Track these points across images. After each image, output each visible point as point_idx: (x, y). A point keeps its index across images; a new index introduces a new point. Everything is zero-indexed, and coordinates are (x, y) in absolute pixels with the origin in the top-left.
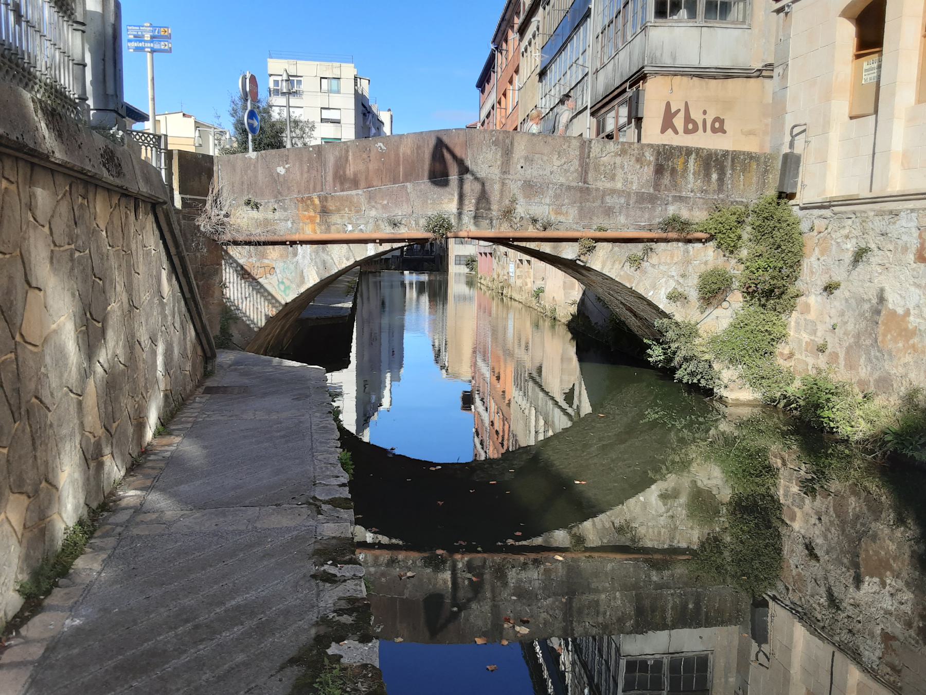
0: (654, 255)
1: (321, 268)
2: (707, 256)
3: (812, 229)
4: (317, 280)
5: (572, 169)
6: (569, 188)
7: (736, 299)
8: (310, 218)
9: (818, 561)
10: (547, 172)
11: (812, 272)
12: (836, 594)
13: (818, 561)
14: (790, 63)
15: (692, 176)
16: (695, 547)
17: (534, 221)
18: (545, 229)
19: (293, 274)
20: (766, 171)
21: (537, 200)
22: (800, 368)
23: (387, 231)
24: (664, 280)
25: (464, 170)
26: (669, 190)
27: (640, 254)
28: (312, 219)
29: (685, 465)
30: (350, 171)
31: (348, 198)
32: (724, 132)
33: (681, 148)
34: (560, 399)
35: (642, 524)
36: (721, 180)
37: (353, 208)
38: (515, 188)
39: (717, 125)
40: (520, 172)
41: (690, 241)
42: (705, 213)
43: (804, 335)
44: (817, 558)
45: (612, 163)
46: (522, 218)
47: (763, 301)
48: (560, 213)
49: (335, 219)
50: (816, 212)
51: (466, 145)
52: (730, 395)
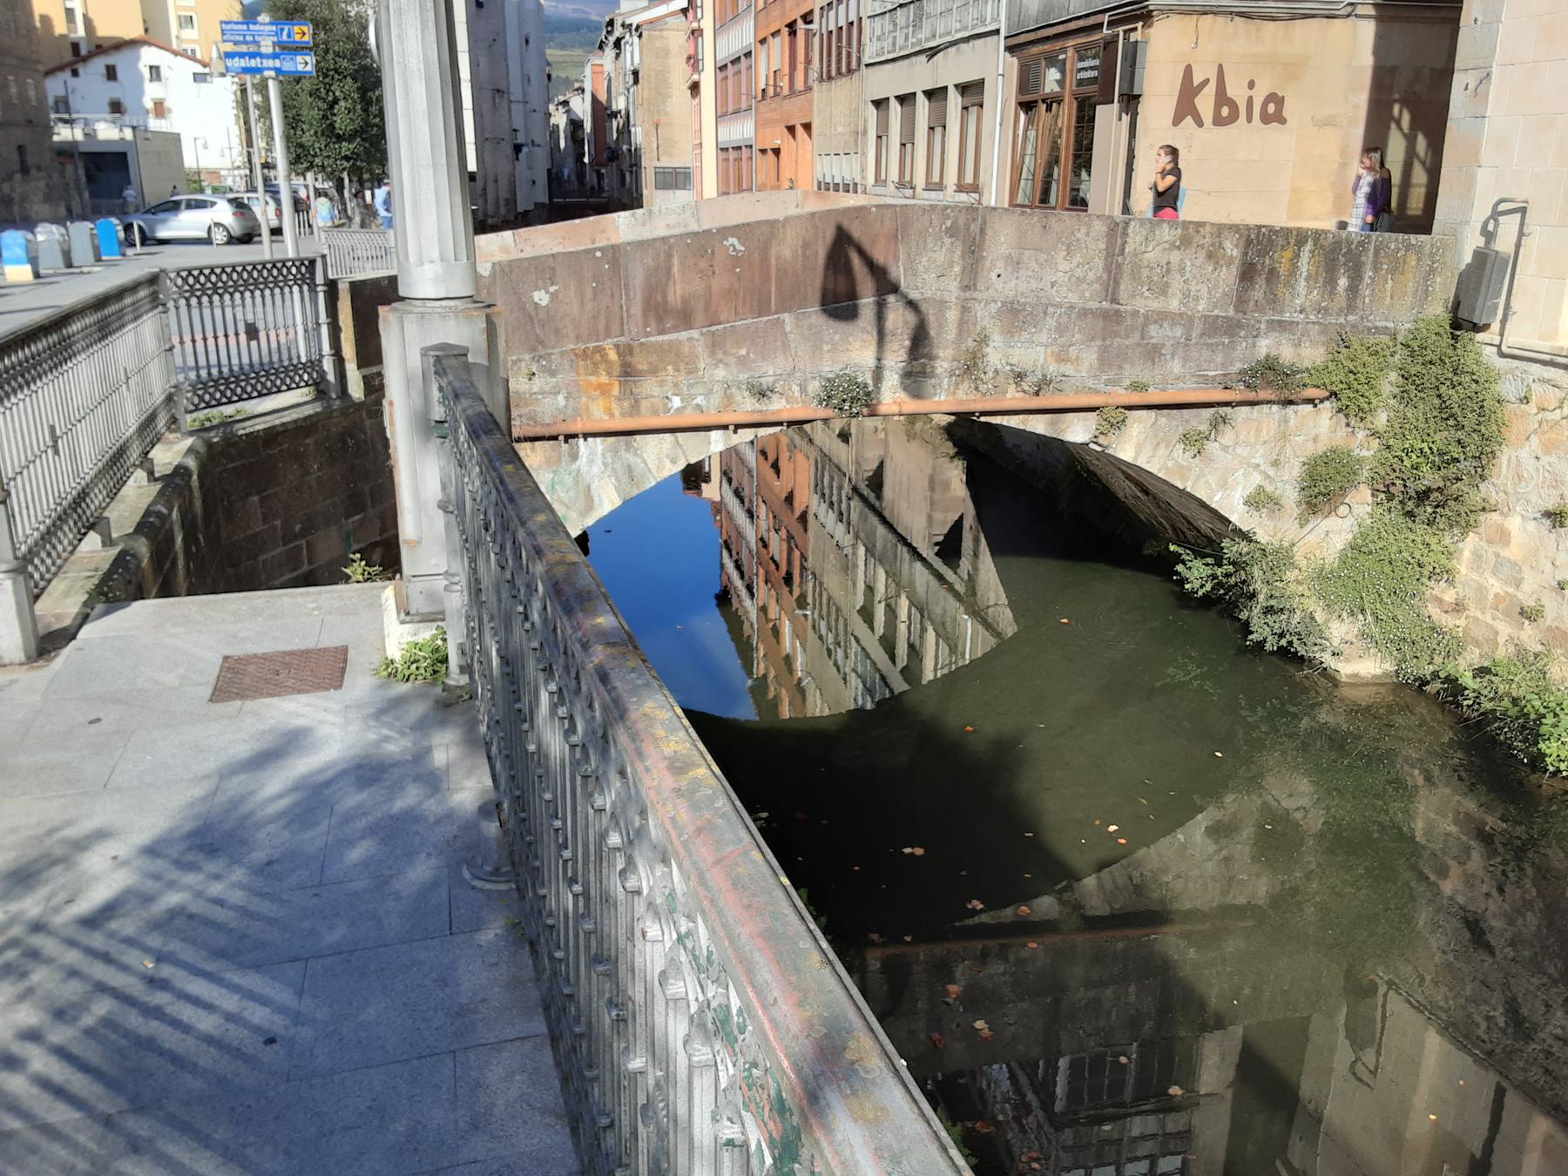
0: (1228, 429)
1: (625, 479)
2: (1318, 428)
3: (1526, 400)
4: (618, 502)
5: (1091, 276)
6: (1085, 312)
7: (1361, 503)
8: (600, 386)
9: (1492, 954)
10: (1046, 284)
11: (1520, 477)
12: (1525, 1011)
13: (1492, 954)
14: (1494, 70)
15: (1303, 283)
16: (1261, 902)
17: (1020, 376)
18: (1037, 394)
19: (572, 494)
20: (1432, 271)
21: (1025, 336)
22: (1478, 633)
23: (747, 407)
24: (1241, 472)
25: (886, 286)
26: (1262, 311)
27: (1204, 428)
28: (604, 390)
29: (1254, 783)
30: (676, 293)
31: (673, 348)
32: (1283, 121)
33: (1288, 231)
34: (928, 552)
35: (1178, 877)
36: (1353, 289)
37: (682, 366)
38: (984, 315)
39: (1271, 108)
40: (1000, 283)
41: (1291, 402)
42: (1322, 350)
43: (1492, 581)
44: (1490, 950)
45: (1163, 262)
46: (996, 371)
47: (1410, 505)
48: (1066, 361)
49: (649, 387)
50: (1536, 369)
51: (895, 237)
52: (1346, 669)
